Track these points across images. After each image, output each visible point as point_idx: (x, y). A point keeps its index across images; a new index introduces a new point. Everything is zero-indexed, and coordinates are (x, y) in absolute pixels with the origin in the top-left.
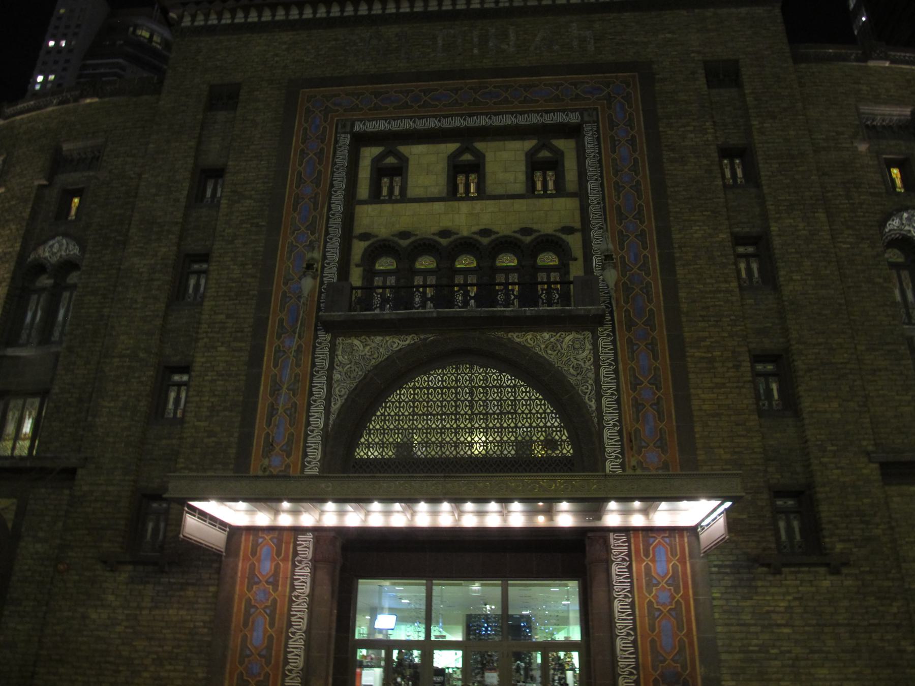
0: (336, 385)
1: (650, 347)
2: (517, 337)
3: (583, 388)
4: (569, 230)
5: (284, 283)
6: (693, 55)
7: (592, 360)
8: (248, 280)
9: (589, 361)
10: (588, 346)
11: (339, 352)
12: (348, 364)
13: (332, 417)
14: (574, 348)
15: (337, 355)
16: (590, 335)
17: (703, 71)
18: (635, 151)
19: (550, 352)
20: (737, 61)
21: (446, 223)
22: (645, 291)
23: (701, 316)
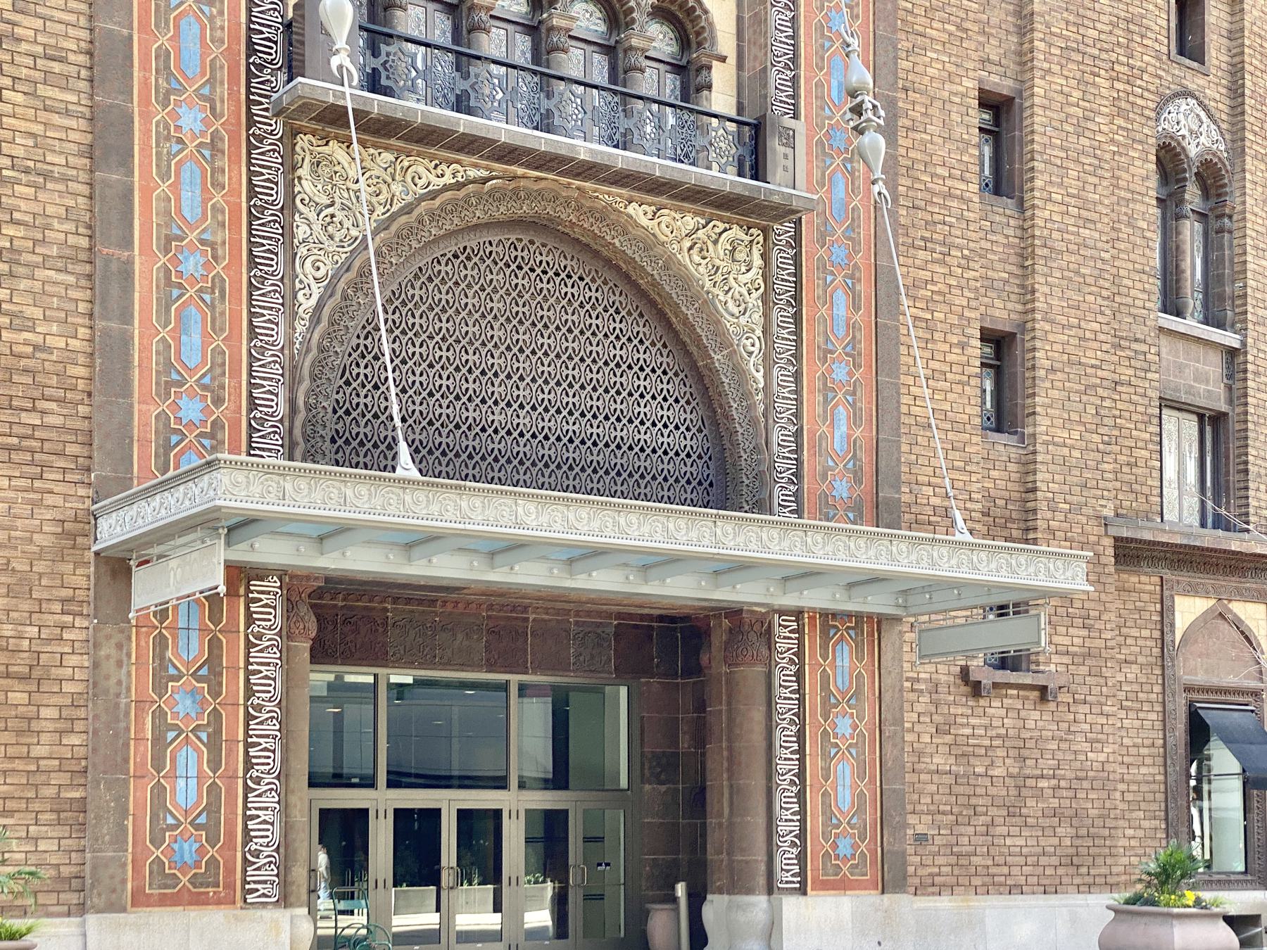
0: (302, 251)
1: (849, 282)
3: (748, 343)
7: (762, 290)
9: (757, 290)
10: (758, 262)
13: (300, 328)
15: (300, 178)
16: (761, 239)
19: (697, 259)
23: (923, 238)
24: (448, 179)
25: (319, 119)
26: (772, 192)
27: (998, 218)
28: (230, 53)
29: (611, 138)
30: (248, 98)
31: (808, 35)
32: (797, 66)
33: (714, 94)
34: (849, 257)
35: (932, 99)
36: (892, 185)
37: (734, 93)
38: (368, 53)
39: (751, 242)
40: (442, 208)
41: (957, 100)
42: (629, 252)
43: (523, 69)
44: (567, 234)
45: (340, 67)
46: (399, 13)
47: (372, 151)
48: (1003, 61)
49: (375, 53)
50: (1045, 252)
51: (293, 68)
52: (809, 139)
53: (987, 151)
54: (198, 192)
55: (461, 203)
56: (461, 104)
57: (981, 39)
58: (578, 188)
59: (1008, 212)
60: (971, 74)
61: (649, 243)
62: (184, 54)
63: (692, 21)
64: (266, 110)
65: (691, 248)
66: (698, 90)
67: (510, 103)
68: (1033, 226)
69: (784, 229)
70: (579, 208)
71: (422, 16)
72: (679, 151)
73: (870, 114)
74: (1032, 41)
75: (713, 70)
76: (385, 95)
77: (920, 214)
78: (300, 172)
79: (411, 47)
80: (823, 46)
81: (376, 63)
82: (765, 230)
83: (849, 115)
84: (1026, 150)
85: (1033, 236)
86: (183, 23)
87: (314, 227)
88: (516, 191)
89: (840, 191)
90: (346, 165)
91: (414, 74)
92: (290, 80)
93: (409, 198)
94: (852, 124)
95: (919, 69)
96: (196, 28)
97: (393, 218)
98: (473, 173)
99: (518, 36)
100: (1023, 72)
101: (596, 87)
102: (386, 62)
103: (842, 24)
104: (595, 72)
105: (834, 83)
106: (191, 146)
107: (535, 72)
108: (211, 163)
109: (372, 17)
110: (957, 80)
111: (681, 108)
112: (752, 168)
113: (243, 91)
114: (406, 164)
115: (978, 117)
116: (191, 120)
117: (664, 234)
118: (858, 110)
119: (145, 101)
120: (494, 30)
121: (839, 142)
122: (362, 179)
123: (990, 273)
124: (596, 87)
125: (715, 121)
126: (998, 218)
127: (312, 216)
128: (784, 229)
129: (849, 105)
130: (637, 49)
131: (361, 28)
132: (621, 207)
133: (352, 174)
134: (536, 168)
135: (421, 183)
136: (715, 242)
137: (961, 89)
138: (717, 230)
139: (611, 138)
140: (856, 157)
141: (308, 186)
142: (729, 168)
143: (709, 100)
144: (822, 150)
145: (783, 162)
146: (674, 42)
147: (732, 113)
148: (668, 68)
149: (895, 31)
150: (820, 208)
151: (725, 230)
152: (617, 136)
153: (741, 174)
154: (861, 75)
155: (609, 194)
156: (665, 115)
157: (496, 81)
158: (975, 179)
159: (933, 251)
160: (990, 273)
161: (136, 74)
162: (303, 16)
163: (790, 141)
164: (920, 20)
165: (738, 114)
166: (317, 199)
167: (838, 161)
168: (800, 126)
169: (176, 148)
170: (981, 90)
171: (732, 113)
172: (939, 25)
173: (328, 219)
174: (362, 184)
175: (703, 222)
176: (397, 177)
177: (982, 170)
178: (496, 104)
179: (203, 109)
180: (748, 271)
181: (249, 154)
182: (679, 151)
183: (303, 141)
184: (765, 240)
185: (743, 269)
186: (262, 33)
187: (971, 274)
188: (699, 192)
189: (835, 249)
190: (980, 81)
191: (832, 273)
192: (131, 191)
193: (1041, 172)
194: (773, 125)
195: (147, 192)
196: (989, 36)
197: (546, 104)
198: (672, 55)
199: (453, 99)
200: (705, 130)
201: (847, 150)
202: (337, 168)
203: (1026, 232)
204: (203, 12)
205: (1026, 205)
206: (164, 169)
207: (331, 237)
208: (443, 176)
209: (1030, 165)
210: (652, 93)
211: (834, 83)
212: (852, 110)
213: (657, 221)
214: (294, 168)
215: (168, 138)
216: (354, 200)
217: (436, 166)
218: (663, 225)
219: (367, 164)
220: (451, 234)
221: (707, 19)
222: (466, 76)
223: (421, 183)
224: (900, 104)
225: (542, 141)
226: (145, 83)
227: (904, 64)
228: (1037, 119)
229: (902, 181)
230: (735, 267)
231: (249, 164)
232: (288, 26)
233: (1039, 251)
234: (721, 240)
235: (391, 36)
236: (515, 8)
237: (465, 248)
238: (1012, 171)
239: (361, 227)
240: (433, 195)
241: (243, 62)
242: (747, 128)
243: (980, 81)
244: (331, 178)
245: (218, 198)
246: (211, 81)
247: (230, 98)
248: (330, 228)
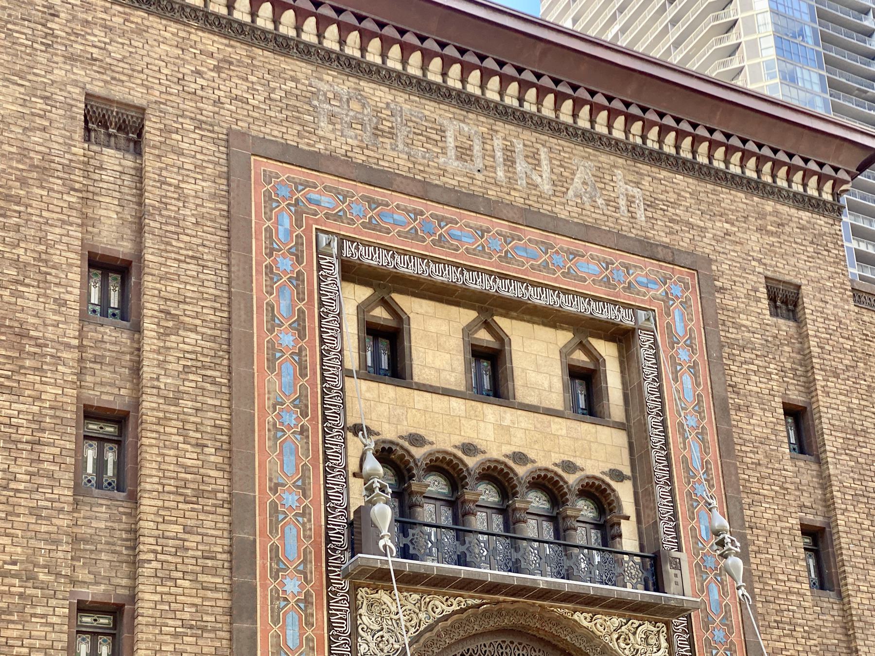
2: (581, 618)
4: (618, 476)
5: (270, 489)
6: (754, 263)
8: (213, 473)
10: (664, 644)
11: (363, 611)
12: (379, 631)
14: (648, 644)
15: (361, 615)
16: (665, 629)
17: (765, 290)
18: (698, 385)
19: (623, 645)
20: (799, 287)
21: (468, 433)
22: (719, 579)
24: (455, 607)
25: (371, 578)
26: (669, 599)
27: (825, 605)
28: (316, 544)
29: (559, 573)
30: (327, 569)
31: (682, 499)
32: (677, 519)
33: (623, 540)
34: (726, 636)
35: (770, 532)
36: (751, 590)
37: (637, 538)
38: (401, 535)
39: (658, 632)
40: (452, 626)
41: (787, 532)
42: (577, 644)
43: (499, 536)
44: (535, 636)
45: (385, 546)
46: (419, 509)
47: (405, 594)
48: (814, 506)
49: (405, 535)
50: (861, 624)
51: (354, 548)
52: (690, 563)
53: (811, 562)
54: (297, 629)
55: (464, 622)
56: (461, 560)
57: (797, 493)
58: (540, 606)
59: (831, 600)
60: (794, 515)
61: (590, 637)
62: (288, 547)
63: (605, 497)
64: (338, 575)
65: (618, 639)
66: (613, 538)
67: (492, 558)
68: (850, 608)
69: (679, 623)
70: (541, 618)
71: (433, 510)
72: (604, 578)
73: (730, 545)
74: (832, 492)
75: (622, 525)
76: (412, 559)
77: (772, 606)
78: (360, 611)
79: (428, 529)
80: (692, 505)
81: (406, 541)
82: (667, 624)
83: (715, 547)
84: (837, 560)
85: (851, 615)
86: (287, 529)
87: (370, 645)
88: (499, 612)
89: (715, 595)
90: (390, 604)
91: (430, 545)
92: (352, 557)
93: (431, 621)
94: (718, 552)
95: (758, 514)
96: (294, 531)
97: (421, 634)
98: (470, 602)
99: (494, 516)
100: (828, 511)
101: (547, 542)
102: (412, 539)
103: (702, 490)
104: (545, 533)
105: (703, 527)
106: (292, 602)
107: (507, 537)
108: (305, 611)
109: (402, 514)
110: (785, 519)
111: (603, 551)
112: (654, 584)
113: (324, 565)
114: (428, 600)
115: (801, 541)
116: (292, 586)
117: (599, 631)
118: (721, 543)
119: (264, 577)
120: (479, 513)
121: (710, 562)
122: (401, 611)
123: (825, 641)
124: (547, 542)
125: (626, 557)
126: (825, 605)
127: (369, 638)
128: (679, 623)
129: (714, 541)
130: (571, 517)
131: (396, 521)
132: (569, 616)
133: (394, 609)
134: (512, 596)
135: (437, 611)
136: (634, 634)
137: (788, 525)
138: (635, 626)
139: (559, 573)
140: (723, 572)
141: (365, 619)
142: (639, 586)
143: (621, 544)
144: (700, 569)
145: (675, 579)
146: (594, 511)
147: (637, 550)
148: (592, 526)
149: (739, 492)
150: (703, 607)
151: (640, 625)
152: (563, 571)
153: (646, 589)
154: (720, 521)
155: (560, 608)
156: (593, 556)
157: (482, 544)
158: (806, 581)
159: (784, 629)
160: (825, 641)
161: (258, 562)
162: (360, 518)
163: (677, 565)
164: (754, 485)
165: (641, 550)
166: (372, 627)
167: (712, 576)
168: (683, 556)
169: (283, 604)
170: (802, 525)
171: (637, 550)
172: (768, 487)
173: (379, 639)
174: (401, 615)
175: (625, 621)
176: (423, 609)
177: (810, 574)
178: (483, 558)
179: (299, 579)
180: (658, 651)
181: (328, 603)
182: (604, 578)
183: (362, 592)
184: (667, 629)
185: (655, 650)
186: (335, 529)
187: (812, 642)
188: (620, 602)
189: (716, 632)
190: (801, 519)
191: (716, 648)
192: (256, 633)
193: (851, 573)
194: (665, 556)
195: (265, 632)
196: (802, 491)
197: (515, 556)
198: (593, 518)
199: (456, 558)
200: (621, 563)
201: (716, 569)
202: (384, 607)
203: (846, 613)
204: (298, 521)
205: (844, 595)
206: (275, 618)
207: (382, 650)
208: (451, 605)
209: (842, 569)
210: (582, 543)
211: (703, 527)
212: (716, 544)
213: (594, 623)
214: (357, 609)
215: (278, 598)
216: (395, 625)
217: (447, 600)
218: (598, 625)
219: (404, 602)
220: (458, 642)
221: (615, 495)
222: (464, 543)
223: (437, 611)
224: (749, 537)
225: (515, 578)
226: (264, 566)
227: (748, 512)
228: (842, 540)
229: (756, 585)
230: (649, 649)
231: (329, 609)
232: (351, 524)
233: (856, 624)
234: (638, 632)
235: (415, 524)
236: (491, 499)
237: (468, 650)
238: (830, 573)
239: (401, 642)
240: (446, 618)
241: (324, 548)
242: (648, 559)
243: (801, 519)
244: (380, 613)
245: (309, 632)
246: (305, 562)
247: (316, 571)
248: (381, 645)
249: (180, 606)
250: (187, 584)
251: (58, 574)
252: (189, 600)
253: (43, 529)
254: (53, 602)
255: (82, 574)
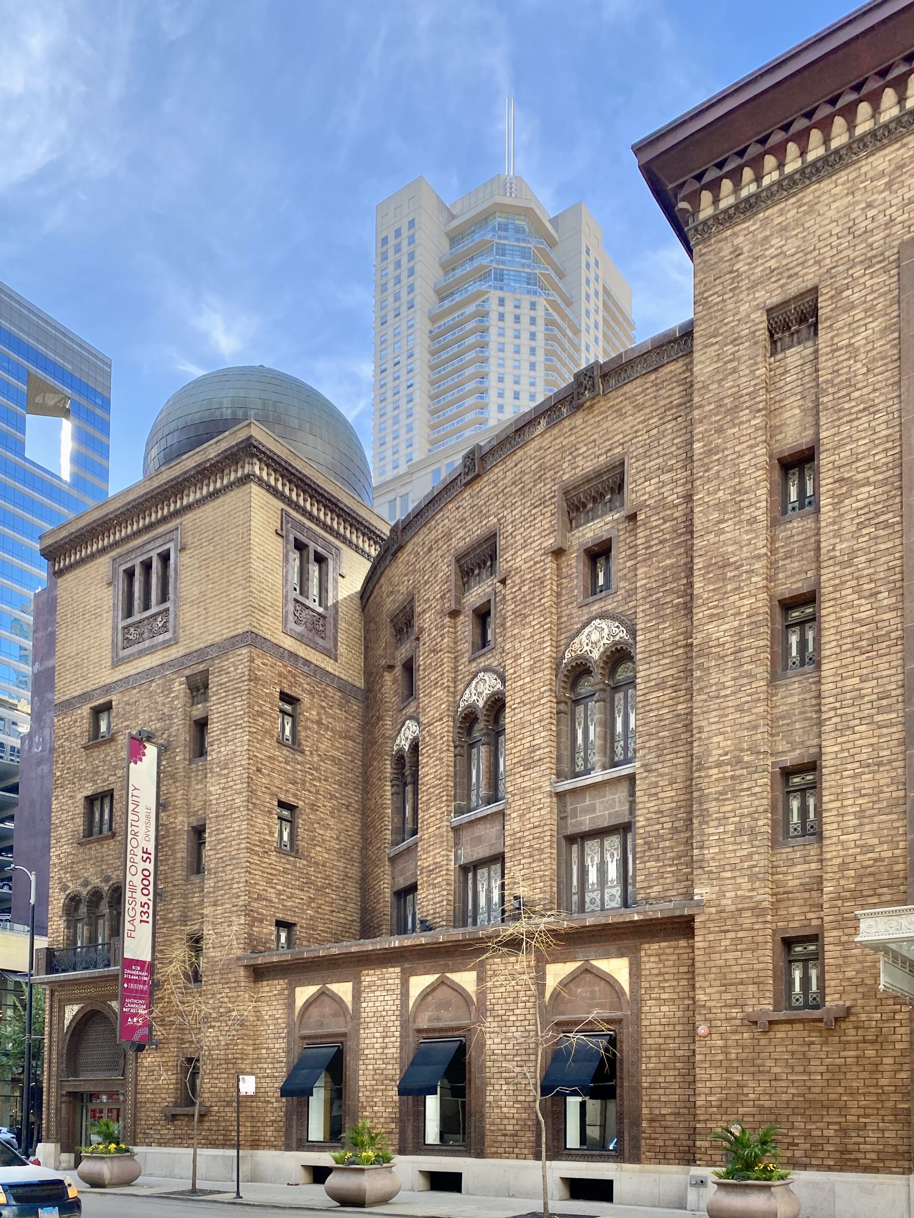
249: (858, 750)
250: (864, 728)
251: (759, 753)
252: (865, 742)
253: (746, 719)
254: (756, 776)
255: (782, 746)
